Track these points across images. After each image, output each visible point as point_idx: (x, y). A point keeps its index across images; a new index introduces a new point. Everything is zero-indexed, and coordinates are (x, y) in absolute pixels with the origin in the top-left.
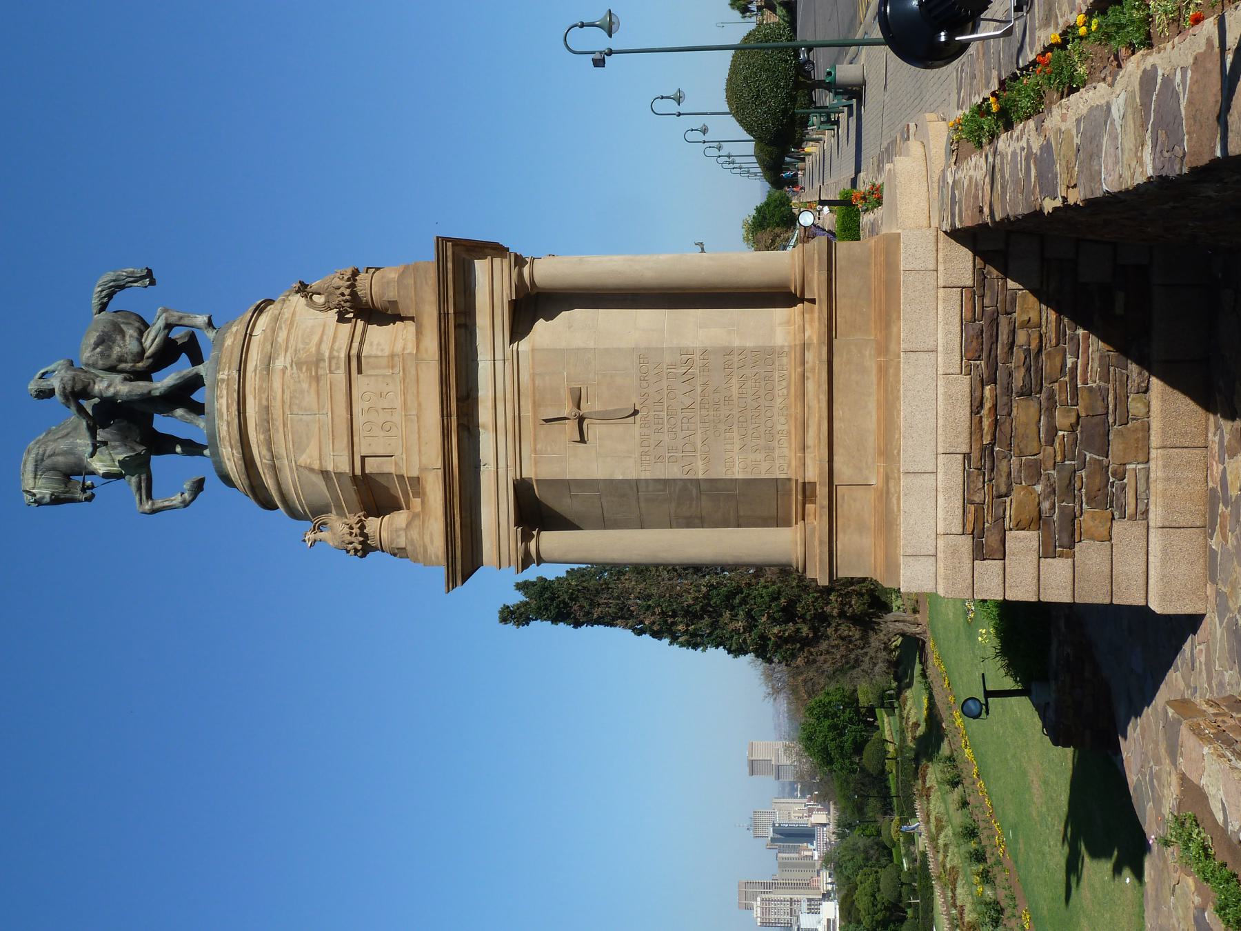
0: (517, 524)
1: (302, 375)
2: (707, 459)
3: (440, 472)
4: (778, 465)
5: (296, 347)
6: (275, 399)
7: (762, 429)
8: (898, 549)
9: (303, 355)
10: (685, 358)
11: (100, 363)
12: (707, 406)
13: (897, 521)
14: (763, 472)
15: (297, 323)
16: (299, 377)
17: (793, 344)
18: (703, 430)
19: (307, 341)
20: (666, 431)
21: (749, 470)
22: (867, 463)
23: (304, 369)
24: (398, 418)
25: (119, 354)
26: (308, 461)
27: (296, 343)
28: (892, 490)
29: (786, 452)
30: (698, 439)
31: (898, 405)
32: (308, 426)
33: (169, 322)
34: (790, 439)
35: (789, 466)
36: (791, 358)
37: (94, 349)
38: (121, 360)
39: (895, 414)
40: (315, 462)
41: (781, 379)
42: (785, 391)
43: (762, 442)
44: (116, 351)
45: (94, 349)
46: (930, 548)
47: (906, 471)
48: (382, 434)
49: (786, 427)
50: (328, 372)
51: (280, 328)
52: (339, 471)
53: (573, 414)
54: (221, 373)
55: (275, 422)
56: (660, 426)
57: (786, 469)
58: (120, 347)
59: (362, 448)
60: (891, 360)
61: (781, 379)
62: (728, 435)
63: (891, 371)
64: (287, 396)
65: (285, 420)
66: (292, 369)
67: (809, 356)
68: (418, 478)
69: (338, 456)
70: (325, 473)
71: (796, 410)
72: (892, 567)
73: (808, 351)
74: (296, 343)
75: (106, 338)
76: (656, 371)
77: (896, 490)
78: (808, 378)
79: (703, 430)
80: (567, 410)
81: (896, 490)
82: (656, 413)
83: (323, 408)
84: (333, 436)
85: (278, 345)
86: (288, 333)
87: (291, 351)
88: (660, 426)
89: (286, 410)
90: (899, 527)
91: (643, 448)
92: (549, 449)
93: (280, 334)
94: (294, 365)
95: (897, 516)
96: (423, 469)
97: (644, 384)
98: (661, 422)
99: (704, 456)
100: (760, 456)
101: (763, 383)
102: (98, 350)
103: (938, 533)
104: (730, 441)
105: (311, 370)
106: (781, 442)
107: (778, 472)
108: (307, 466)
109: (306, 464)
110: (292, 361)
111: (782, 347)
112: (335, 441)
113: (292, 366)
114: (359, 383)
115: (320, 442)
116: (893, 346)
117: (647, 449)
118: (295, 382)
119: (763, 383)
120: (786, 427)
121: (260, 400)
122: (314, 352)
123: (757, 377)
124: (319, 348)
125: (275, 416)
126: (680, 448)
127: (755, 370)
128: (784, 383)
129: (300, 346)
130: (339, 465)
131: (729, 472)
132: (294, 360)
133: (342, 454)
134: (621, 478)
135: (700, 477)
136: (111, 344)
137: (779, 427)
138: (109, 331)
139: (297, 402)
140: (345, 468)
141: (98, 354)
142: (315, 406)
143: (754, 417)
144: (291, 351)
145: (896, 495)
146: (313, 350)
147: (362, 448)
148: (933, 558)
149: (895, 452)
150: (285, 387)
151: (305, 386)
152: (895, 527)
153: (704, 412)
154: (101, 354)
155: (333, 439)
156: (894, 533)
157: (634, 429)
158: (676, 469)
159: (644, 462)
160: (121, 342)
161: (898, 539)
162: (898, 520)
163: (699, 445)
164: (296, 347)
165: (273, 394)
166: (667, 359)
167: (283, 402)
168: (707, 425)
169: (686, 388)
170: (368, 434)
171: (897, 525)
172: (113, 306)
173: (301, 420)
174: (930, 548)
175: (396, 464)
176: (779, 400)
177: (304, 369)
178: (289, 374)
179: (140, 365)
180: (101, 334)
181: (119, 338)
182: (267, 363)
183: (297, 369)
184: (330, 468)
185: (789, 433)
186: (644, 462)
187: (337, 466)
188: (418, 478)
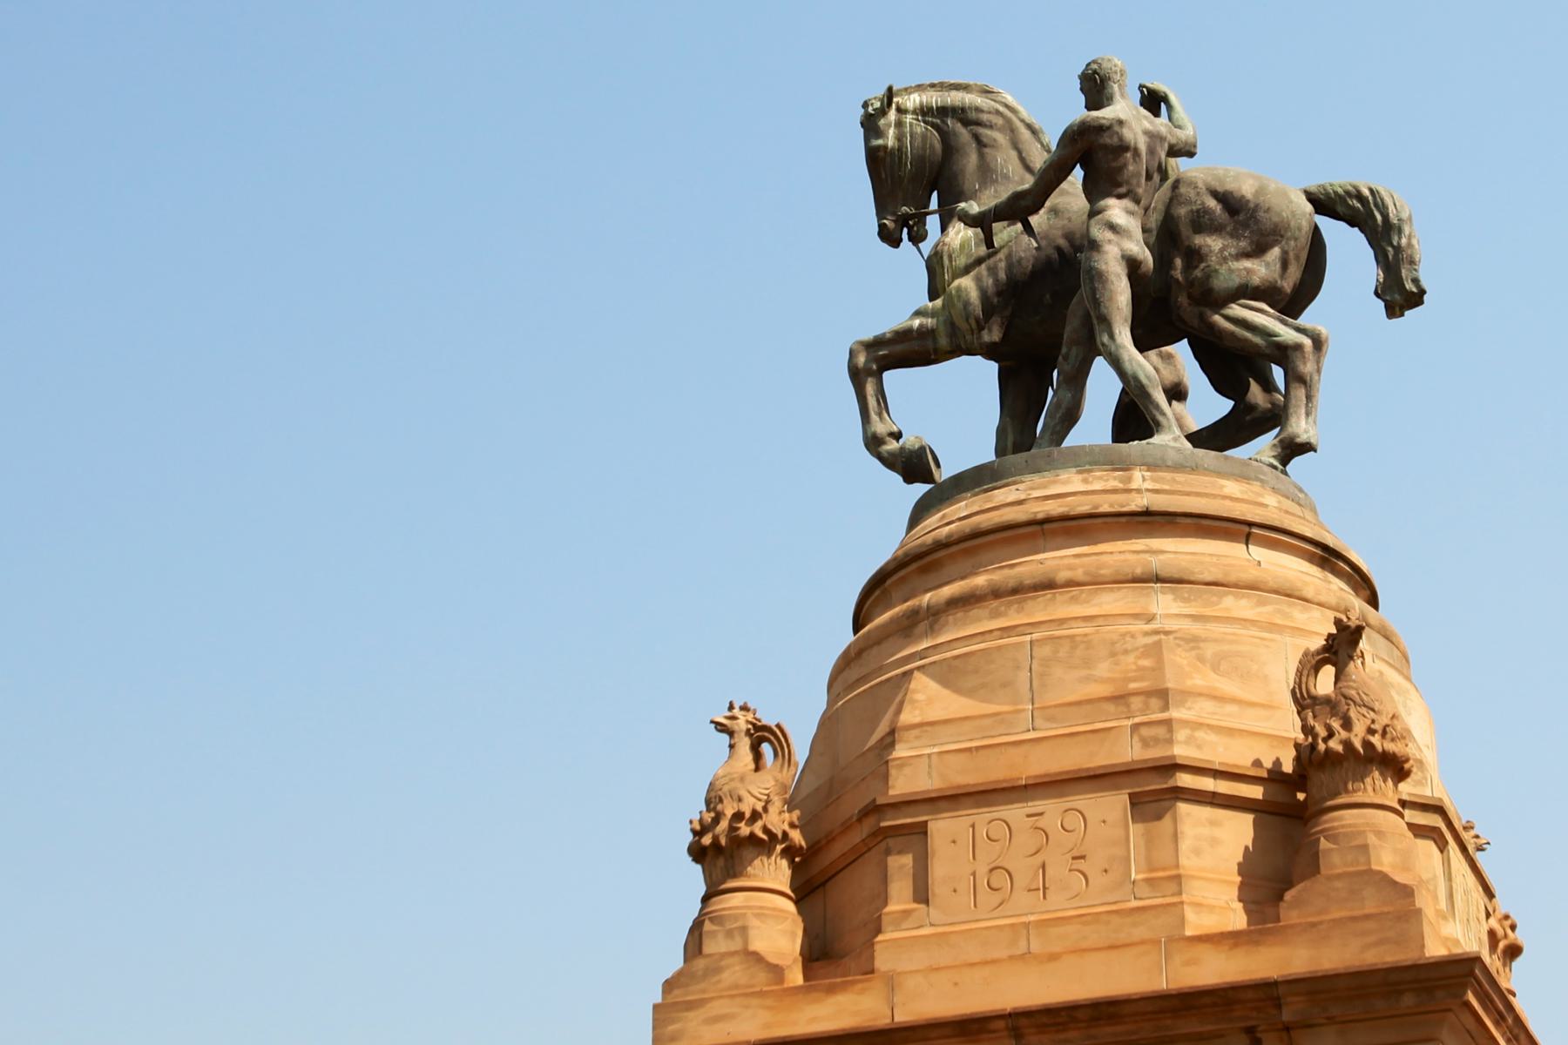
1: (1131, 658)
3: (883, 1021)
5: (1205, 640)
6: (1074, 600)
9: (1178, 661)
11: (1182, 211)
15: (1272, 640)
16: (1126, 652)
19: (1224, 666)
23: (1146, 663)
24: (1025, 907)
25: (1205, 250)
26: (920, 697)
27: (1216, 641)
32: (1005, 685)
33: (1290, 352)
37: (1215, 194)
38: (1194, 256)
40: (917, 712)
44: (1213, 244)
45: (1215, 194)
48: (982, 870)
50: (1137, 720)
51: (1261, 603)
52: (893, 772)
54: (1147, 474)
55: (1016, 606)
58: (1222, 250)
59: (944, 828)
64: (1079, 630)
65: (1021, 628)
66: (1147, 634)
68: (872, 972)
69: (930, 766)
70: (889, 740)
74: (1216, 641)
75: (1241, 217)
83: (1050, 719)
84: (978, 748)
85: (1215, 599)
86: (1245, 620)
87: (1196, 628)
89: (1043, 628)
93: (1244, 602)
94: (1156, 638)
96: (891, 983)
102: (1212, 203)
105: (1141, 679)
108: (908, 697)
109: (915, 691)
110: (1167, 633)
112: (967, 754)
113: (1157, 632)
114: (1112, 805)
115: (966, 718)
118: (1113, 643)
121: (1070, 568)
122: (1189, 683)
124: (1200, 695)
125: (1030, 604)
129: (1209, 650)
130: (907, 770)
132: (1171, 637)
133: (934, 774)
136: (1228, 229)
138: (1257, 221)
139: (1061, 654)
140: (902, 784)
141: (1203, 203)
142: (1053, 697)
144: (1196, 628)
146: (1198, 681)
147: (944, 828)
150: (1100, 621)
151: (1103, 669)
154: (1206, 211)
155: (969, 750)
160: (1233, 251)
164: (1205, 640)
165: (1084, 595)
167: (1061, 622)
170: (982, 832)
172: (1329, 226)
173: (1018, 668)
175: (906, 913)
177: (1146, 663)
178: (1132, 628)
179: (1183, 300)
180: (1252, 205)
181: (1243, 244)
182: (1163, 573)
183: (1145, 646)
184: (900, 751)
187: (901, 766)
188: (872, 972)
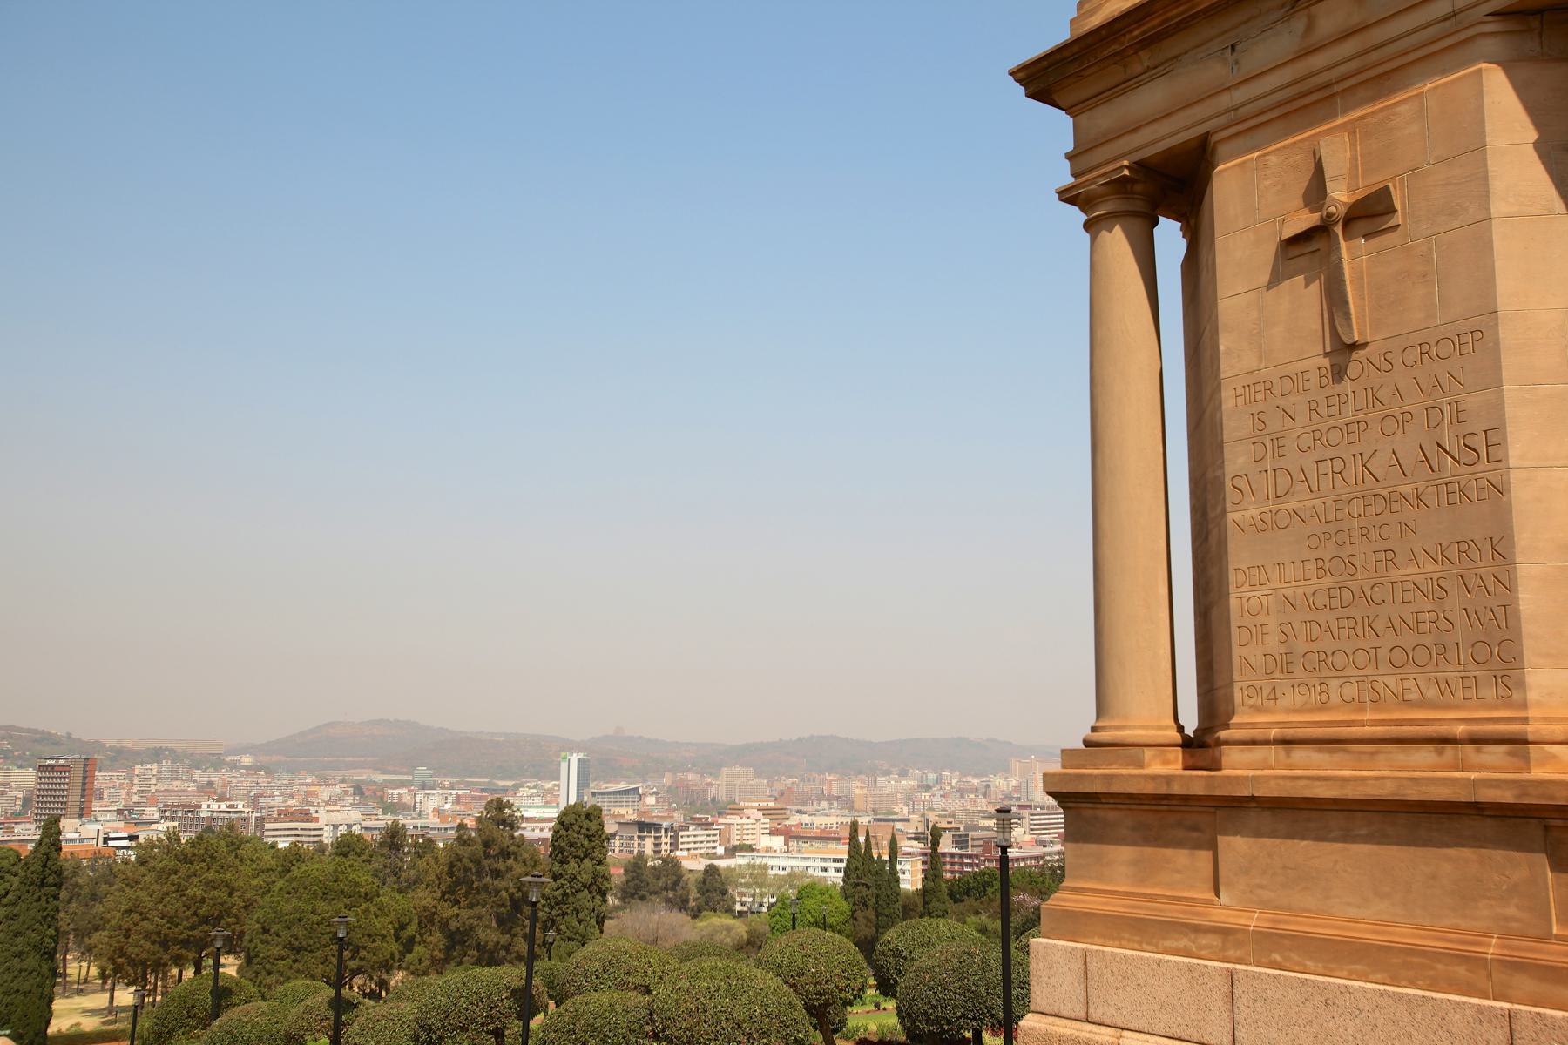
0: (1140, 166)
2: (1262, 527)
4: (1257, 684)
7: (1327, 644)
8: (1101, 941)
10: (1479, 442)
12: (1371, 510)
13: (1148, 944)
14: (1244, 651)
17: (1532, 713)
18: (1321, 510)
20: (1314, 428)
21: (1247, 621)
22: (1261, 887)
28: (1205, 940)
29: (1285, 702)
30: (1300, 501)
31: (1379, 977)
34: (1311, 711)
35: (1258, 709)
36: (1495, 707)
39: (1358, 967)
41: (1443, 686)
42: (1413, 696)
43: (1301, 646)
46: (1100, 1011)
47: (1235, 977)
49: (1335, 698)
53: (1333, 209)
56: (1323, 410)
57: (1251, 701)
60: (1490, 975)
61: (1443, 686)
62: (1312, 566)
63: (1461, 971)
67: (1495, 754)
71: (1369, 722)
72: (1076, 925)
73: (1510, 754)
76: (1445, 379)
77: (1201, 948)
78: (1440, 753)
79: (1321, 510)
80: (1340, 195)
81: (1201, 948)
82: (1351, 396)
88: (1323, 410)
90: (1137, 947)
91: (1276, 381)
92: (1268, 183)
95: (1157, 946)
97: (1413, 355)
98: (1334, 410)
99: (1267, 518)
100: (1273, 642)
101: (1428, 640)
103: (1125, 1033)
104: (1300, 574)
106: (1304, 690)
107: (1245, 685)
111: (1521, 684)
116: (1526, 984)
117: (1276, 391)
119: (1428, 640)
120: (1335, 698)
123: (1444, 625)
126: (1282, 463)
127: (1458, 616)
128: (1432, 693)
131: (1241, 577)
134: (1222, 348)
135: (1230, 516)
137: (1334, 684)
143: (1352, 623)
145: (1194, 949)
148: (1082, 1015)
149: (1277, 957)
152: (1137, 938)
153: (1357, 506)
156: (1127, 936)
157: (1316, 361)
158: (1241, 460)
159: (1252, 391)
161: (1117, 943)
162: (1150, 948)
163: (1289, 506)
166: (1472, 401)
168: (1331, 516)
169: (1409, 456)
171: (1140, 943)
174: (1100, 1011)
176: (1392, 682)
185: (1324, 707)
186: (1252, 391)
